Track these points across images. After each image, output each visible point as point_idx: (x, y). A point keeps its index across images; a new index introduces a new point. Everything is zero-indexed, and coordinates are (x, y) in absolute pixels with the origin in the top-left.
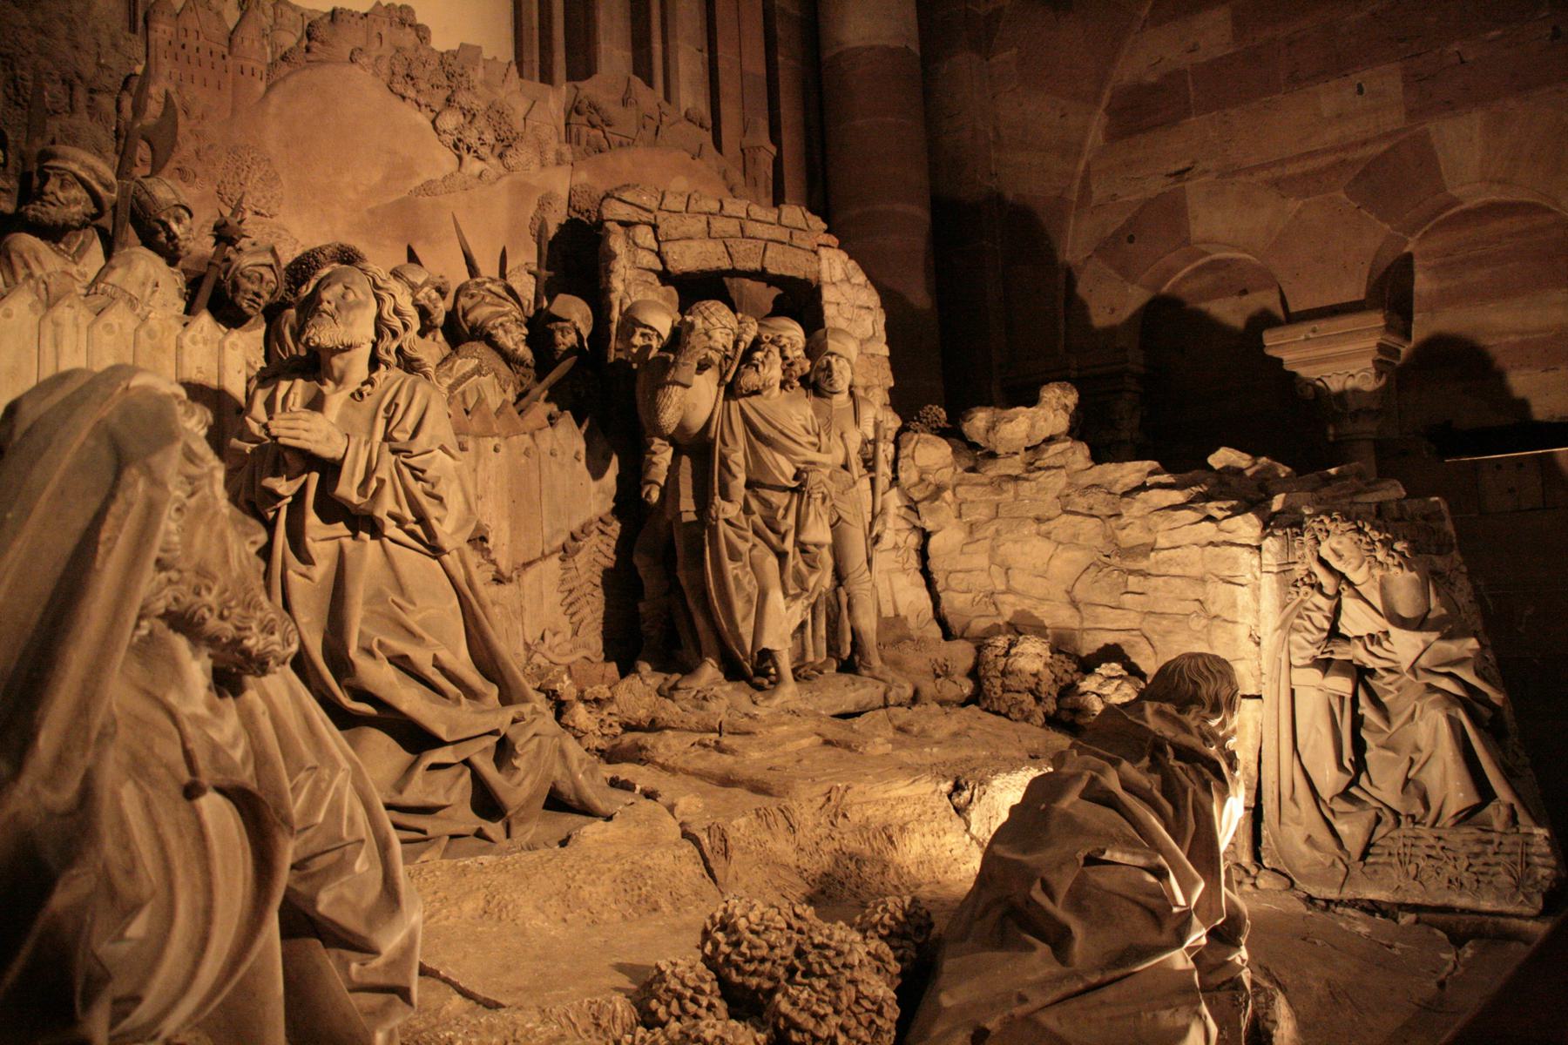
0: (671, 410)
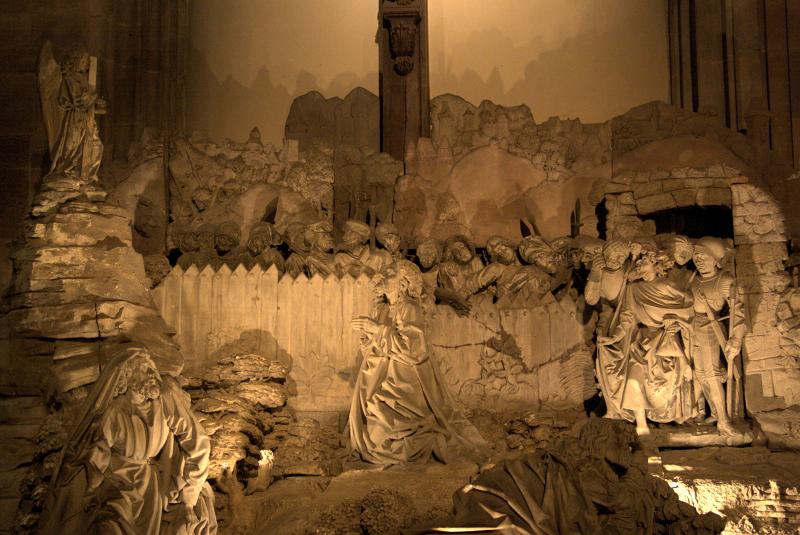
0: (590, 293)
